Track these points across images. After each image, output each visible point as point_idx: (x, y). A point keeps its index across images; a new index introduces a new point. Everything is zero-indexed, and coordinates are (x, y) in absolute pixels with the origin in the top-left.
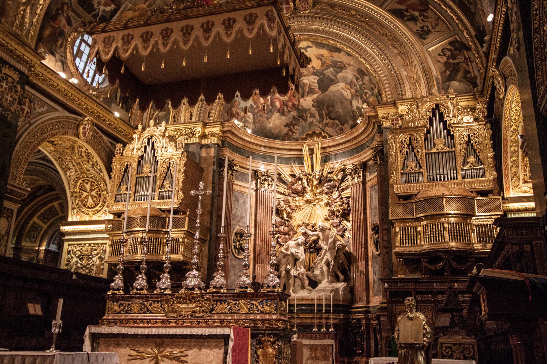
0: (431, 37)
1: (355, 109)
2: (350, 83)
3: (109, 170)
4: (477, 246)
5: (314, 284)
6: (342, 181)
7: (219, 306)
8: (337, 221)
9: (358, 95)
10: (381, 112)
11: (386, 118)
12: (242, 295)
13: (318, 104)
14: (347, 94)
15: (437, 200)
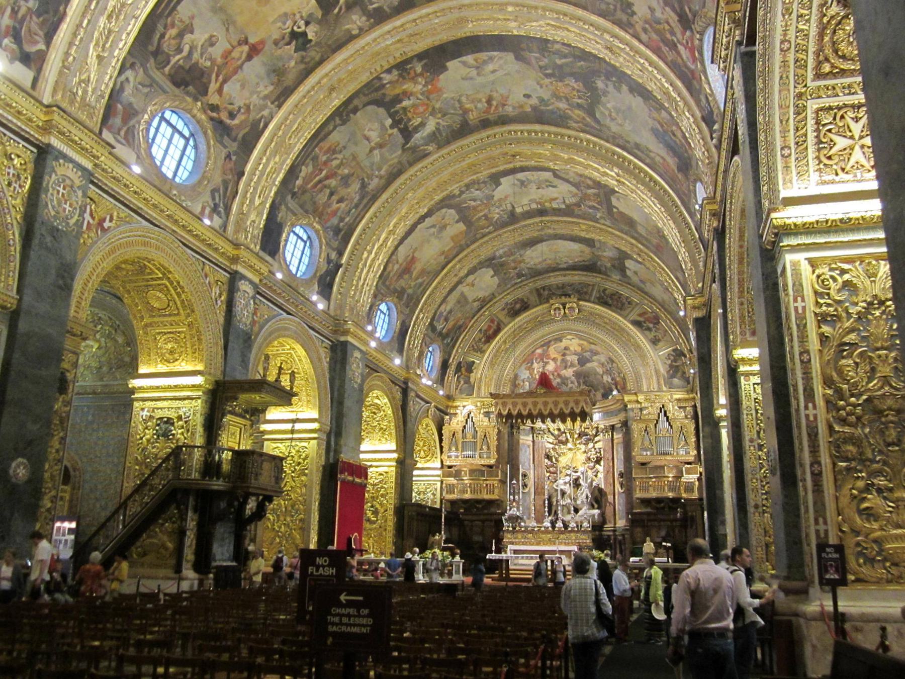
0: (661, 344)
1: (605, 381)
2: (603, 364)
3: (440, 435)
4: (684, 495)
5: (576, 510)
6: (596, 436)
7: (562, 536)
8: (592, 464)
9: (608, 372)
10: (627, 398)
11: (629, 402)
12: (572, 531)
13: (578, 375)
14: (600, 370)
15: (662, 467)
